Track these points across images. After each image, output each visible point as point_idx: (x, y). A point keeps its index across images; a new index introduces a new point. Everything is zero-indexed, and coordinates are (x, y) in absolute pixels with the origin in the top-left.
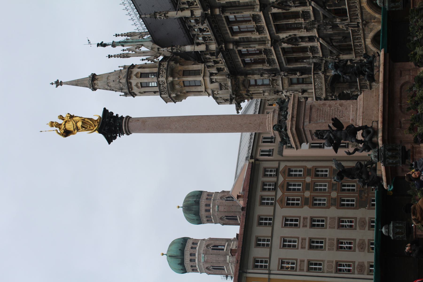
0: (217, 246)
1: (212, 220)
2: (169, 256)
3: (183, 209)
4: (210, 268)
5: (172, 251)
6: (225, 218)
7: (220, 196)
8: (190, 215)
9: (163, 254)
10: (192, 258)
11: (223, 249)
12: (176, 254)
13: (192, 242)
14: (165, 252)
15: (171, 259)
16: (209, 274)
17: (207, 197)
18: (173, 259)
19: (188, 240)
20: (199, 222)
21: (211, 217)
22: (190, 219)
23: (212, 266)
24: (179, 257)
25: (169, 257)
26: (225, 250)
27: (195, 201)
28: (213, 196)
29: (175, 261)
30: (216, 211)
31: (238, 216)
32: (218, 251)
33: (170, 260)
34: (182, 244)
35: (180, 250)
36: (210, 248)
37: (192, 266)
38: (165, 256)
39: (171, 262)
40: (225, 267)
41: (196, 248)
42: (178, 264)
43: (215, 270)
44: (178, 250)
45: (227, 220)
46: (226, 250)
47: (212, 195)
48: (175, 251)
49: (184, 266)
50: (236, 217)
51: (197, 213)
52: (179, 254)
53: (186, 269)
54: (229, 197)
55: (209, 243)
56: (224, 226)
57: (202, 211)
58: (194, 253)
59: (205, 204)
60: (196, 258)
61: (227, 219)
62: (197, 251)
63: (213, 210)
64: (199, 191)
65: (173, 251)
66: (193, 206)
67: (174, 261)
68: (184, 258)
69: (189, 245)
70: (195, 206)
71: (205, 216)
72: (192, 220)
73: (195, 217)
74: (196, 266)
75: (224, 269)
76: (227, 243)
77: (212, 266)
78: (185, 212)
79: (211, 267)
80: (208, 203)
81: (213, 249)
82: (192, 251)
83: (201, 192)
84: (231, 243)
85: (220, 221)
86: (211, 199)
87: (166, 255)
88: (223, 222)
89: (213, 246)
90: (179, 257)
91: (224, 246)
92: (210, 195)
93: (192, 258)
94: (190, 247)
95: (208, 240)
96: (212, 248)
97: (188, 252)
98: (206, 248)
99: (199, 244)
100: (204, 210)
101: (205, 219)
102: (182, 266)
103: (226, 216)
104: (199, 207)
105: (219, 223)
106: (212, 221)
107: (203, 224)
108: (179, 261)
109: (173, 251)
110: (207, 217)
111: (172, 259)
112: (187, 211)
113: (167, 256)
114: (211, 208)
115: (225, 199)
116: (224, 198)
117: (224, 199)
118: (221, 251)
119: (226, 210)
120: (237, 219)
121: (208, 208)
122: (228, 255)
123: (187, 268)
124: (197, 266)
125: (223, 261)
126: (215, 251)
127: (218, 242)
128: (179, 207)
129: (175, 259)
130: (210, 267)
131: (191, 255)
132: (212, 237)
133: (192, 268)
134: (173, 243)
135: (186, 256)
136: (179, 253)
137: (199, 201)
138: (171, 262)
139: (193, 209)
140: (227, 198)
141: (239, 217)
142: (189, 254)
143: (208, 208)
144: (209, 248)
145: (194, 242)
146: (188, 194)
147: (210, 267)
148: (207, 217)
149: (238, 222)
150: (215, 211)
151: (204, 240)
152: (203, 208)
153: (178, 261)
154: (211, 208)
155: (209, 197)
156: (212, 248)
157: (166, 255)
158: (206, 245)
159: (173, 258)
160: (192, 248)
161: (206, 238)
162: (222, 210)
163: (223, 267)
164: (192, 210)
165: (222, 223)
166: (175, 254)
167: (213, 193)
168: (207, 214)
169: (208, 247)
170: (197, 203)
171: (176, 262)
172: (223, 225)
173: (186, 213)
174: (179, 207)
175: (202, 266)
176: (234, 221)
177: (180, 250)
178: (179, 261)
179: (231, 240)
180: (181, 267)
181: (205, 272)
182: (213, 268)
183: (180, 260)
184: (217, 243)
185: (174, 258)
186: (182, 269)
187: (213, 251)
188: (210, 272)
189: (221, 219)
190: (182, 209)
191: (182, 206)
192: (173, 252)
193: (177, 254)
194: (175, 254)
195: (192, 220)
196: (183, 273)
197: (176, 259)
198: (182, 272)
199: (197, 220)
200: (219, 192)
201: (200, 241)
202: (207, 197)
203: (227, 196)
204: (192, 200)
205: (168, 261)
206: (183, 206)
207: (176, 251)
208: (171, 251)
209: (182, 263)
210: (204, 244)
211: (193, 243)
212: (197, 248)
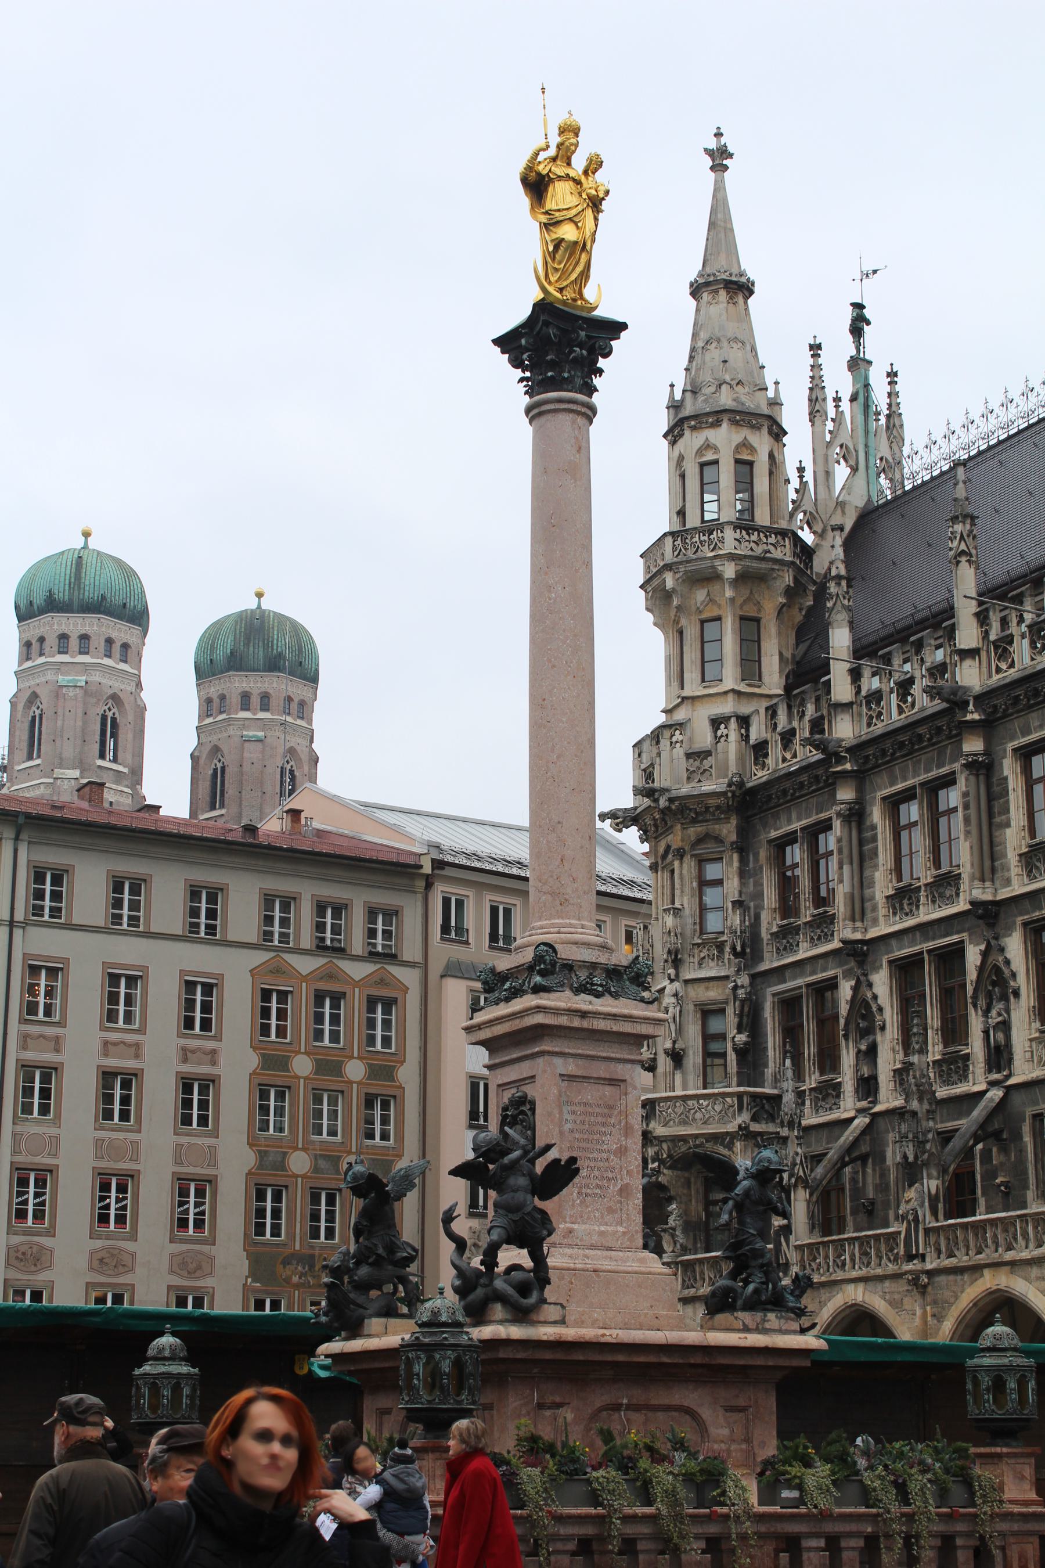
0: (113, 735)
1: (211, 715)
3: (252, 610)
4: (34, 708)
5: (98, 568)
6: (219, 765)
7: (298, 748)
8: (231, 638)
9: (87, 535)
10: (74, 643)
11: (102, 756)
12: (87, 583)
13: (130, 642)
14: (93, 543)
15: (69, 564)
16: (13, 704)
17: (296, 700)
18: (68, 572)
19: (136, 630)
20: (205, 670)
21: (221, 713)
22: (215, 637)
23: (41, 716)
24: (76, 593)
25: (76, 556)
26: (100, 762)
27: (280, 655)
28: (299, 722)
29: (62, 579)
30: (245, 733)
31: (223, 811)
32: (98, 738)
33: (64, 562)
34: (125, 604)
35: (103, 597)
36: (110, 709)
37: (42, 640)
38: (78, 543)
39: (59, 564)
40: (38, 761)
41: (110, 656)
42: (50, 591)
43: (26, 726)
44: (102, 592)
45: (210, 772)
46: (99, 767)
47: (302, 718)
48: (97, 578)
49: (42, 611)
50: (222, 806)
51: (236, 663)
52: (86, 594)
53: (30, 618)
54: (293, 778)
55: (126, 705)
57: (245, 679)
58: (92, 649)
59: (271, 691)
60: (72, 657)
61: (215, 770)
62: (99, 661)
63: (247, 722)
64: (317, 671)
65: (98, 573)
66: (261, 649)
67: (63, 575)
68: (73, 612)
69: (121, 631)
70: (261, 653)
71: (225, 692)
72: (213, 642)
73: (221, 654)
74: (41, 654)
75: (30, 757)
76: (126, 770)
77: (41, 716)
78: (241, 620)
79: (38, 712)
80: (273, 703)
81: (104, 718)
82: (98, 643)
83: (313, 679)
84: (127, 786)
85: (207, 749)
86: (289, 714)
87: (85, 547)
88: (204, 756)
89: (114, 720)
90: (76, 593)
91: (115, 760)
92: (304, 710)
93: (74, 643)
94: (114, 635)
95: (139, 702)
96: (110, 714)
97: (95, 628)
98: (110, 692)
99: (122, 666)
100: (247, 689)
101: (214, 690)
102: (43, 603)
103: (223, 769)
105: (200, 744)
106: (208, 716)
107: (198, 685)
108: (62, 594)
109: (98, 573)
110: (223, 697)
111: (69, 568)
113: (80, 550)
114: (255, 714)
115: (289, 767)
116: (292, 763)
117: (288, 762)
118: (97, 747)
119: (247, 767)
120: (213, 807)
121: (255, 701)
122: (81, 772)
124: (42, 660)
125: (61, 753)
126: (98, 727)
127: (130, 736)
128: (259, 595)
129: (68, 577)
131: (84, 638)
132: (148, 715)
133: (34, 642)
134: (128, 574)
135: (80, 621)
136: (90, 593)
137: (280, 671)
138: (59, 564)
139: (251, 649)
140: (292, 772)
142: (86, 629)
143: (255, 701)
144: (110, 705)
145: (129, 652)
146: (307, 631)
148: (223, 697)
149: (204, 812)
150: (244, 727)
151: (139, 685)
152: (255, 683)
153: (61, 590)
154: (255, 714)
155: (294, 706)
156: (110, 714)
157: (85, 547)
158: (120, 694)
159: (73, 570)
160: (109, 641)
161: (146, 696)
162: (246, 755)
163: (39, 757)
165: (200, 751)
166: (88, 578)
167: (310, 721)
168: (235, 699)
169: (110, 702)
170: (274, 664)
171: (57, 582)
172: (192, 755)
173: (236, 622)
174: (259, 595)
175: (43, 680)
176: (208, 799)
177: (103, 597)
178: (61, 595)
179: (138, 787)
180: (39, 600)
181: (19, 690)
182: (34, 718)
183: (66, 598)
184: (126, 734)
185: (73, 575)
187: (99, 719)
188: (20, 707)
189: (216, 750)
190: (254, 606)
191: (263, 608)
192: (93, 570)
193: (87, 588)
195: (213, 642)
197: (67, 582)
198: (22, 606)
200: (313, 746)
201: (136, 672)
202: (296, 700)
203: (296, 773)
204: (283, 644)
205: (63, 553)
206: (265, 611)
207: (97, 583)
208: (99, 564)
209: (52, 605)
210: (123, 687)
211: (125, 646)
212: (107, 661)
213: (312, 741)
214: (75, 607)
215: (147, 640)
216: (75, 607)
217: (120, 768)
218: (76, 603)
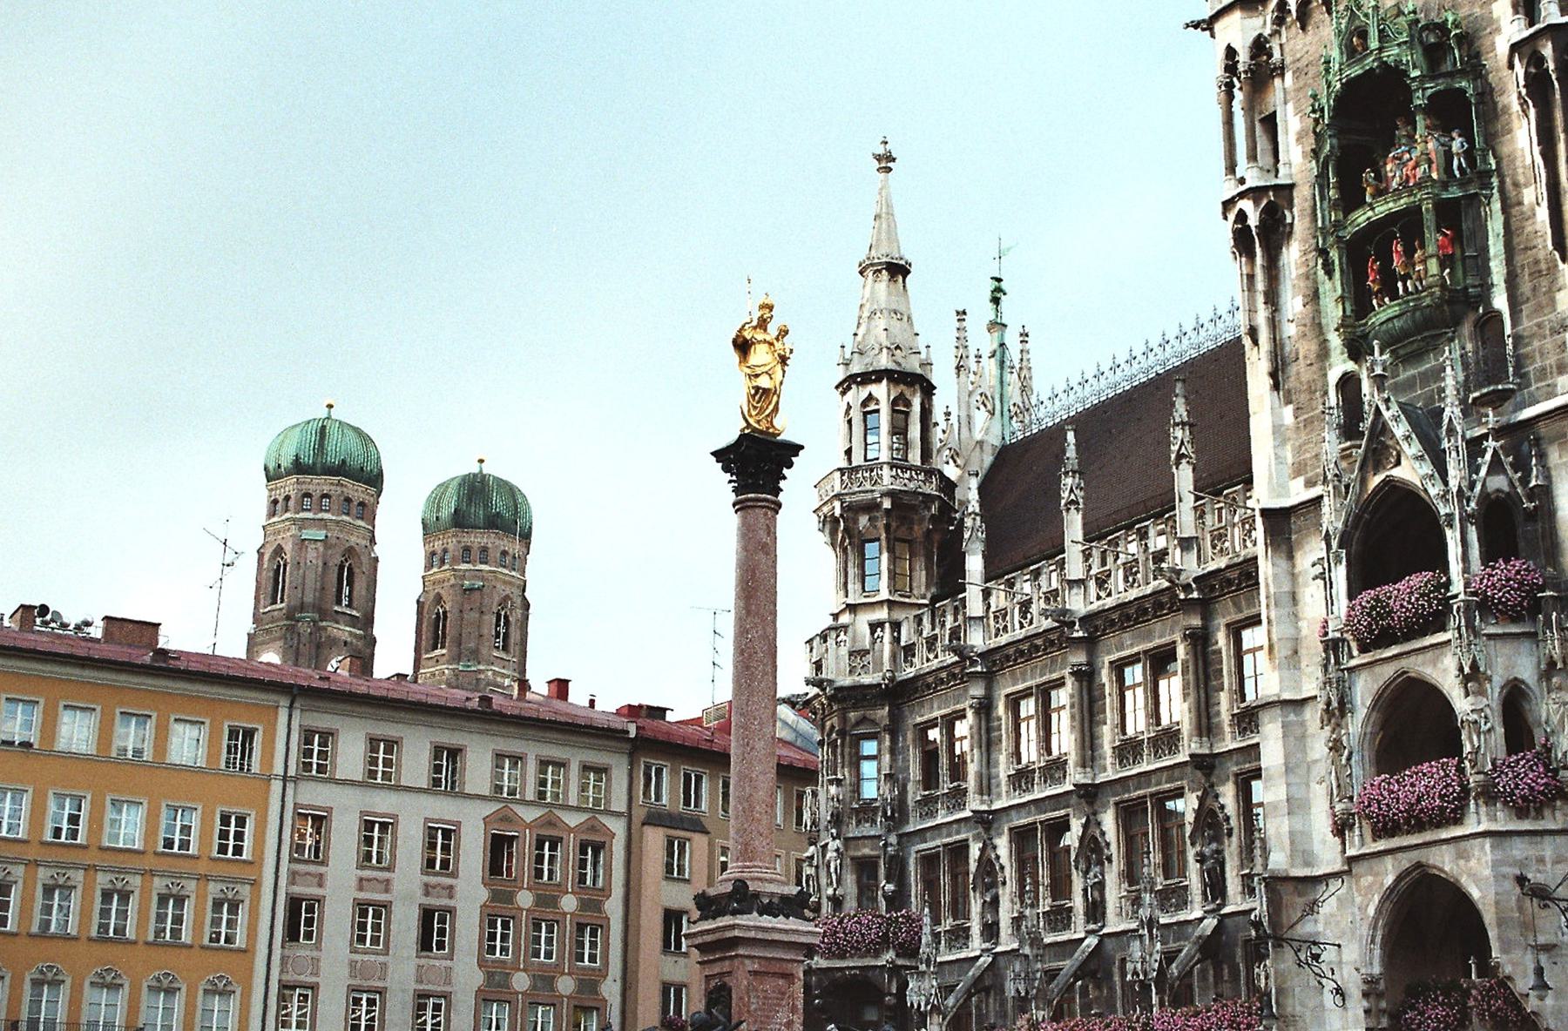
0: (350, 584)
2: (323, 427)
3: (475, 475)
11: (339, 602)
14: (335, 414)
18: (313, 439)
19: (372, 490)
23: (285, 566)
24: (319, 459)
26: (336, 608)
31: (444, 651)
34: (362, 468)
37: (287, 498)
38: (323, 413)
40: (279, 606)
42: (297, 456)
46: (336, 611)
49: (289, 473)
50: (442, 647)
56: (415, 606)
69: (357, 491)
73: (447, 512)
75: (274, 602)
77: (285, 566)
79: (282, 563)
81: (341, 568)
83: (526, 537)
85: (431, 596)
86: (504, 567)
90: (319, 459)
91: (349, 606)
92: (519, 563)
103: (445, 613)
104: (480, 528)
108: (307, 459)
112: (468, 494)
115: (503, 613)
121: (475, 554)
123: (280, 483)
129: (312, 444)
130: (282, 558)
133: (280, 500)
134: (365, 439)
136: (332, 458)
140: (506, 617)
141: (443, 655)
143: (475, 554)
147: (282, 558)
151: (373, 541)
152: (477, 539)
161: (378, 550)
163: (282, 602)
164: (469, 505)
167: (523, 573)
170: (494, 523)
172: (418, 601)
174: (481, 461)
177: (344, 461)
180: (286, 462)
182: (279, 566)
184: (360, 585)
186: (279, 466)
187: (336, 569)
188: (266, 557)
189: (439, 599)
190: (476, 470)
191: (484, 472)
194: (330, 447)
195: (439, 501)
196: (266, 469)
199: (437, 518)
201: (370, 528)
204: (498, 503)
205: (309, 422)
209: (299, 467)
211: (362, 504)
213: (524, 591)
214: (319, 471)
215: (380, 499)
216: (319, 471)
217: (354, 613)
218: (319, 465)
